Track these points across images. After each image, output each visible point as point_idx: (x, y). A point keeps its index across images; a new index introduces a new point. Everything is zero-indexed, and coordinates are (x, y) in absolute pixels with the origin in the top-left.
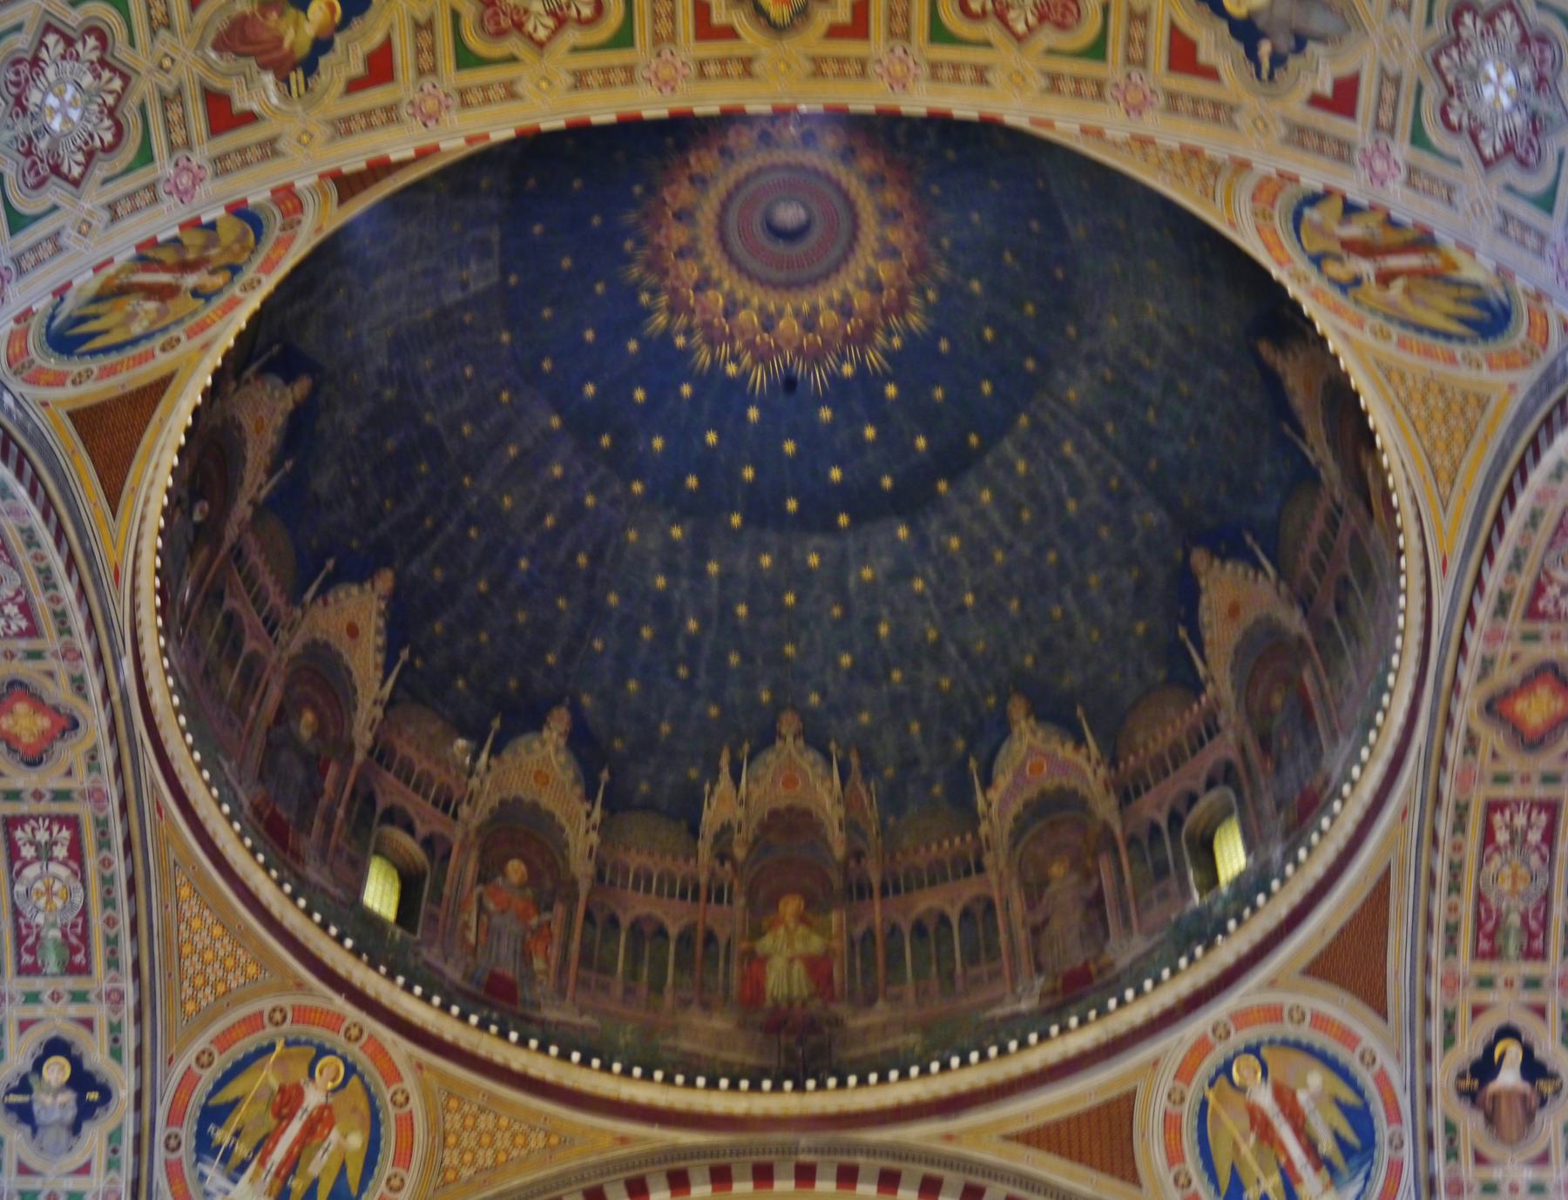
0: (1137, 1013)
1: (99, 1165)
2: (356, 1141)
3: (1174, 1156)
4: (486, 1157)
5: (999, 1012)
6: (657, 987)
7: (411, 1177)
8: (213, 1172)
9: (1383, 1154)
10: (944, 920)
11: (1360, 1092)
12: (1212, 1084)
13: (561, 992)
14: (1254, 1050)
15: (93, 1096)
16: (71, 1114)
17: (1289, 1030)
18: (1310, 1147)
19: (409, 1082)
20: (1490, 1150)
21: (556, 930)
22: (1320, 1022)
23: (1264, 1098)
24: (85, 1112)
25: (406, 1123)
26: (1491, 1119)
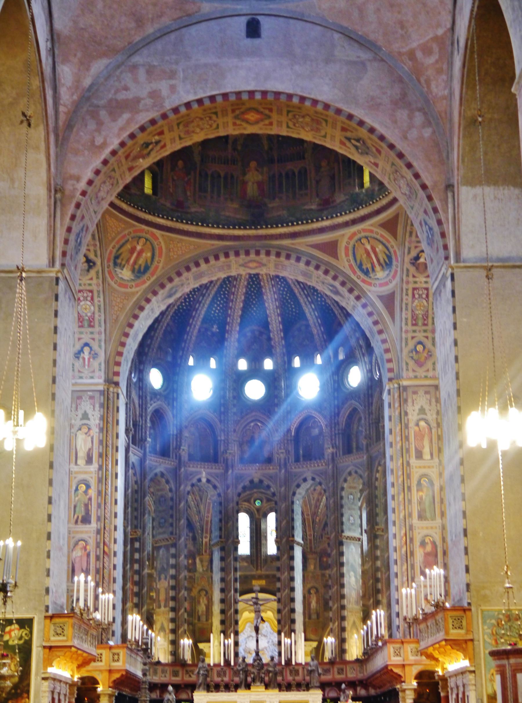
0: (340, 220)
1: (94, 278)
2: (149, 255)
3: (347, 255)
4: (180, 252)
5: (306, 207)
6: (219, 196)
7: (162, 260)
8: (118, 270)
9: (394, 267)
10: (294, 174)
11: (390, 253)
12: (356, 242)
13: (195, 202)
14: (366, 238)
15: (91, 264)
16: (87, 268)
17: (375, 235)
18: (378, 260)
19: (161, 240)
20: (416, 274)
21: (192, 181)
22: (382, 236)
23: (369, 247)
24: (90, 267)
25: (161, 249)
26: (417, 268)
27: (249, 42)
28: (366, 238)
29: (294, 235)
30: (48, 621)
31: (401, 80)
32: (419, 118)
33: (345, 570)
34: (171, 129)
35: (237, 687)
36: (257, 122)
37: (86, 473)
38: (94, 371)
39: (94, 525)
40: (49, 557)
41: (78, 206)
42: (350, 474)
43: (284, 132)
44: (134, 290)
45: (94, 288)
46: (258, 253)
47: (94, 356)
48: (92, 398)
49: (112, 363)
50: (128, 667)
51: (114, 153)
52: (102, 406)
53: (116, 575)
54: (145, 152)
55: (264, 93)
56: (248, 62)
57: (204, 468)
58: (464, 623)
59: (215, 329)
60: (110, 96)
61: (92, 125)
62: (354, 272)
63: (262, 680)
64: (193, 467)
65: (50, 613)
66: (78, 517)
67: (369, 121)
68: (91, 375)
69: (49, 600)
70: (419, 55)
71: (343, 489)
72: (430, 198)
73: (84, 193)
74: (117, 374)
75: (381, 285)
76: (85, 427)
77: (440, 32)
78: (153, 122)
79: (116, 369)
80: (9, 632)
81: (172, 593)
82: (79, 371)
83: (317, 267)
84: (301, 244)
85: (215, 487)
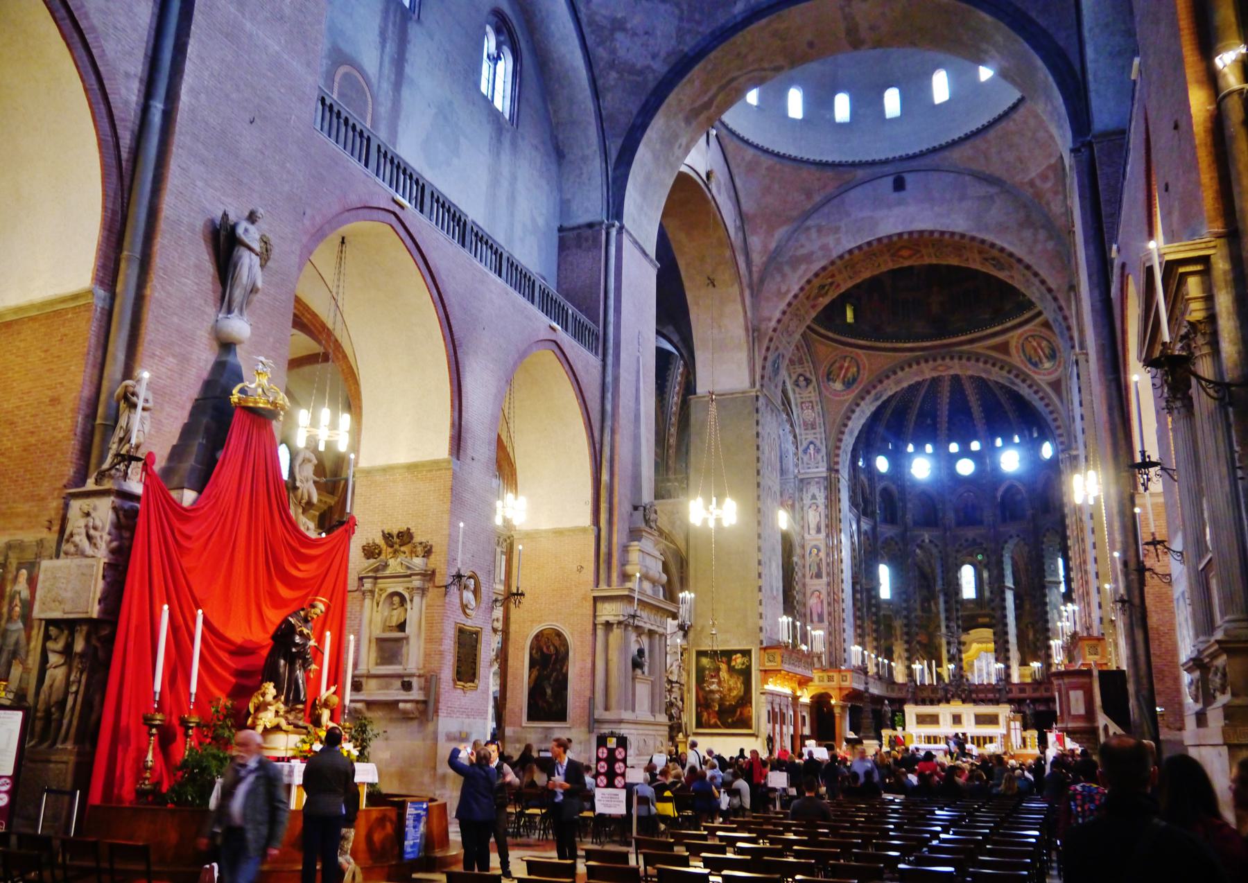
2: (855, 369)
3: (1018, 352)
8: (831, 384)
14: (1032, 336)
27: (896, 195)
28: (1032, 336)
29: (972, 341)
30: (762, 652)
31: (1025, 206)
32: (1042, 235)
33: (1048, 608)
34: (840, 272)
35: (939, 702)
36: (910, 257)
37: (817, 540)
39: (825, 579)
40: (761, 604)
41: (771, 340)
42: (1048, 530)
43: (934, 261)
44: (846, 397)
45: (813, 399)
46: (943, 358)
47: (818, 451)
48: (818, 483)
49: (832, 454)
50: (855, 686)
51: (796, 296)
52: (826, 488)
53: (845, 617)
54: (823, 292)
55: (911, 233)
56: (896, 211)
58: (1099, 650)
59: (929, 421)
60: (791, 254)
61: (778, 278)
62: (1026, 367)
63: (960, 697)
65: (765, 645)
67: (998, 242)
69: (762, 636)
70: (1038, 182)
71: (1043, 543)
72: (1055, 299)
73: (775, 330)
74: (837, 463)
75: (1049, 374)
77: (1053, 161)
78: (824, 269)
79: (836, 459)
80: (735, 659)
81: (905, 630)
83: (994, 365)
84: (978, 347)
85: (936, 546)
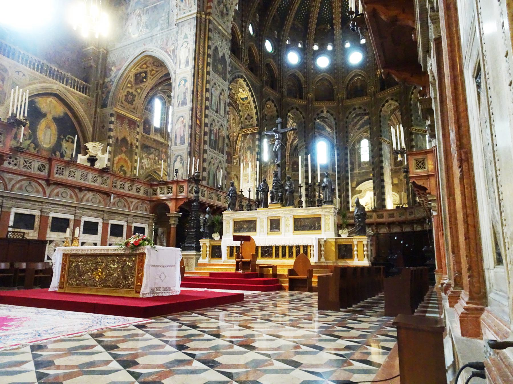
38: (191, 7)
48: (190, 23)
57: (325, 104)
59: (329, 27)
64: (318, 104)
66: (180, 102)
68: (190, 9)
76: (186, 43)
82: (183, 10)
85: (332, 115)
